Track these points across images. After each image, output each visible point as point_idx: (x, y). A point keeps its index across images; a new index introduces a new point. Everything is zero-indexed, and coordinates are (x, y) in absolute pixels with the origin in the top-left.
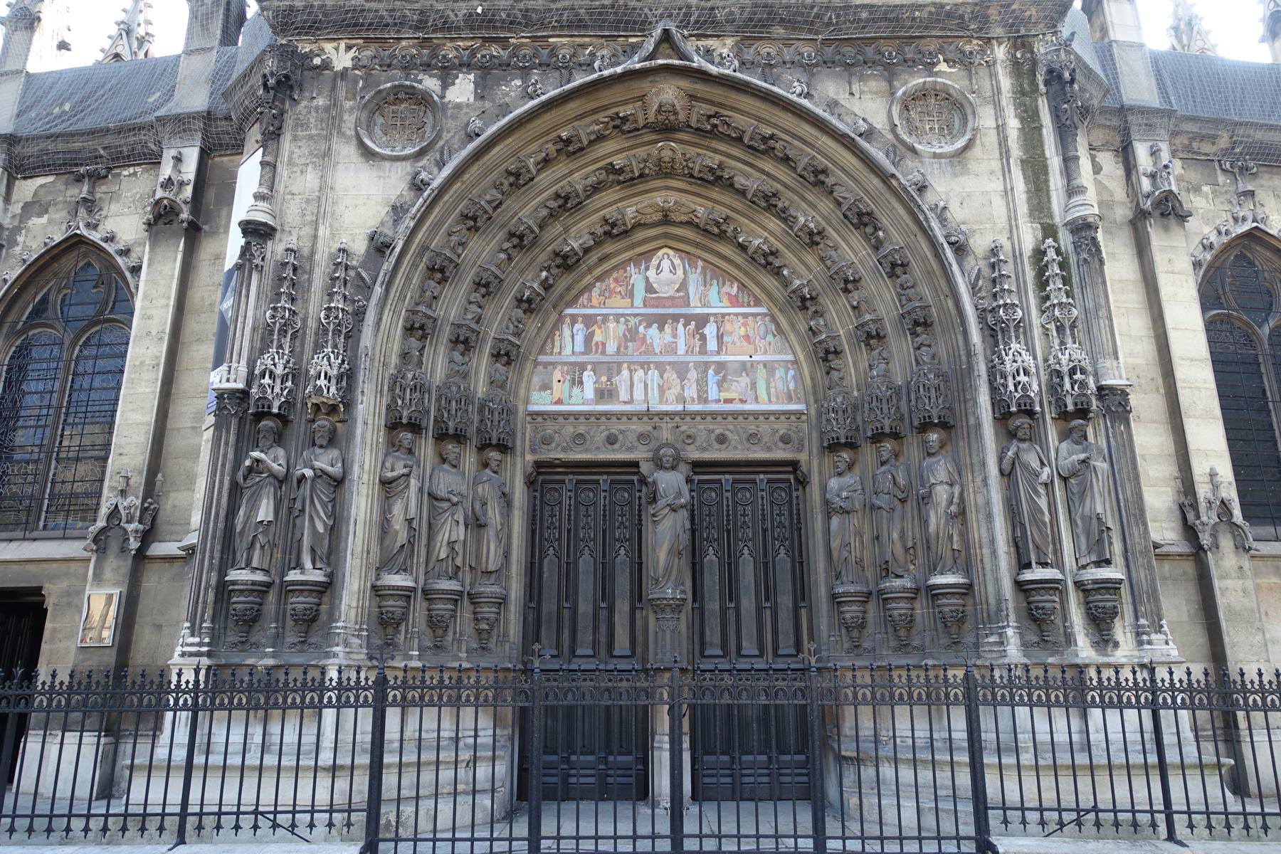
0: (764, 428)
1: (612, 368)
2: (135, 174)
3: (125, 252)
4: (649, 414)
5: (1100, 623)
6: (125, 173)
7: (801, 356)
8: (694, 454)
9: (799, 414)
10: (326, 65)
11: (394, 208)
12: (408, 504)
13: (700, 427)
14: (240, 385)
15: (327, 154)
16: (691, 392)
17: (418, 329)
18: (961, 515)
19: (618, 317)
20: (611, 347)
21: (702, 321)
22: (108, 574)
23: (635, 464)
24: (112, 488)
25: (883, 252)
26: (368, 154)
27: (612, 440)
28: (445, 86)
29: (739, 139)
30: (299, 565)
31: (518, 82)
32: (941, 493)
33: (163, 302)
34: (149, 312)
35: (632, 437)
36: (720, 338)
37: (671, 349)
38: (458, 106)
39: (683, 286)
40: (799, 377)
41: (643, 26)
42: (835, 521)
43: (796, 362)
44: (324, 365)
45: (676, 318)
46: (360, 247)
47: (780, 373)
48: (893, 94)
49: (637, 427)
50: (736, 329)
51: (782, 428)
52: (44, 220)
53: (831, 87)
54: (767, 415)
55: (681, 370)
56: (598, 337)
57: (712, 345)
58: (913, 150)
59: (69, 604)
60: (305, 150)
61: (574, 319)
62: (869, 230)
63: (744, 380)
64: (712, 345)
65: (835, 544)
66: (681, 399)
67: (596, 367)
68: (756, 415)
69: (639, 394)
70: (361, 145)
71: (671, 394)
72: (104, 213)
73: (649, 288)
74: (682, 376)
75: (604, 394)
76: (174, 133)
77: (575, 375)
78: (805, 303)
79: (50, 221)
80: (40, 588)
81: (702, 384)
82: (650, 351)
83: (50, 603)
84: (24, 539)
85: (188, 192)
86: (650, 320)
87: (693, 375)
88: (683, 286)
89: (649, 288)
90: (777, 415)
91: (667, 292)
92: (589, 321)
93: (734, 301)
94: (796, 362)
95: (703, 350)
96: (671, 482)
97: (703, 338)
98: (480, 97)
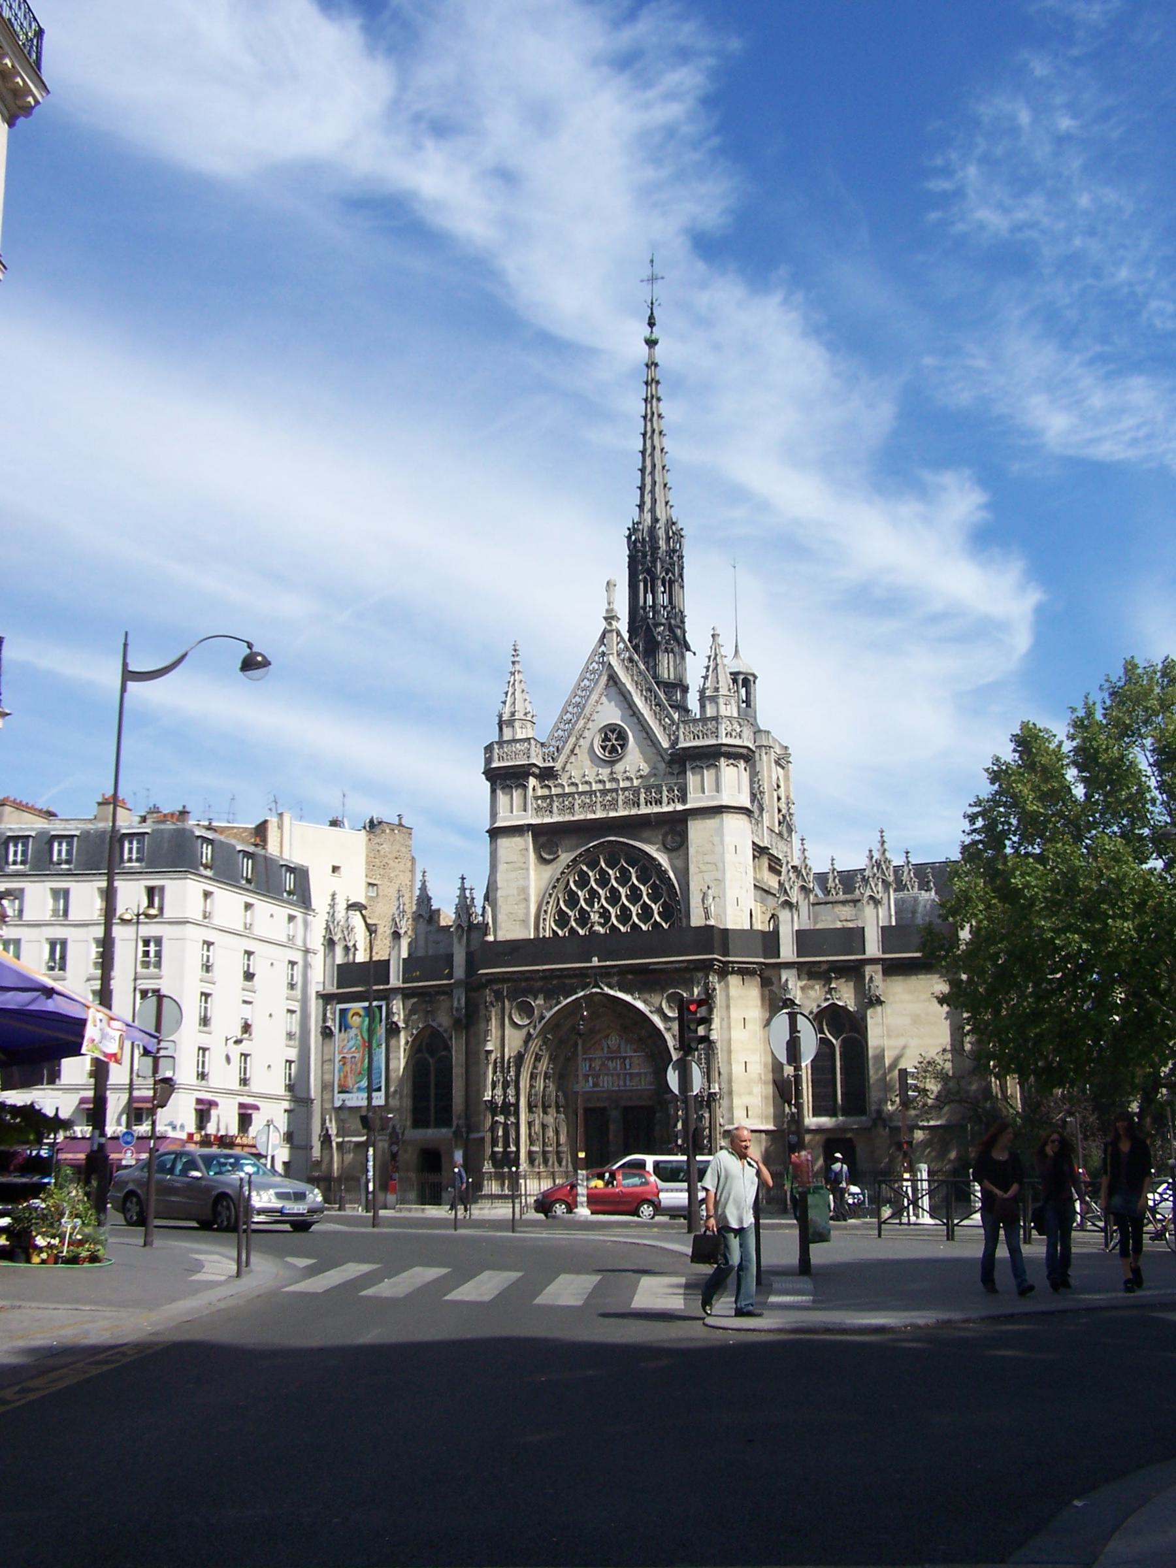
1: (597, 1076)
3: (446, 1031)
12: (537, 1127)
14: (489, 1098)
16: (621, 1083)
17: (533, 1077)
20: (597, 1068)
21: (625, 1058)
30: (509, 1147)
37: (615, 1069)
39: (619, 1046)
44: (511, 1091)
45: (617, 1058)
50: (636, 1061)
52: (416, 1016)
53: (647, 996)
55: (618, 1075)
57: (628, 1067)
61: (585, 1059)
64: (628, 1067)
66: (619, 1086)
67: (594, 1076)
69: (606, 1085)
71: (616, 1084)
73: (609, 1047)
74: (619, 1078)
75: (595, 1085)
77: (586, 1076)
82: (609, 1070)
86: (609, 1059)
87: (622, 1077)
88: (619, 1046)
89: (609, 1047)
92: (591, 1059)
93: (635, 1052)
95: (625, 1069)
96: (615, 1114)
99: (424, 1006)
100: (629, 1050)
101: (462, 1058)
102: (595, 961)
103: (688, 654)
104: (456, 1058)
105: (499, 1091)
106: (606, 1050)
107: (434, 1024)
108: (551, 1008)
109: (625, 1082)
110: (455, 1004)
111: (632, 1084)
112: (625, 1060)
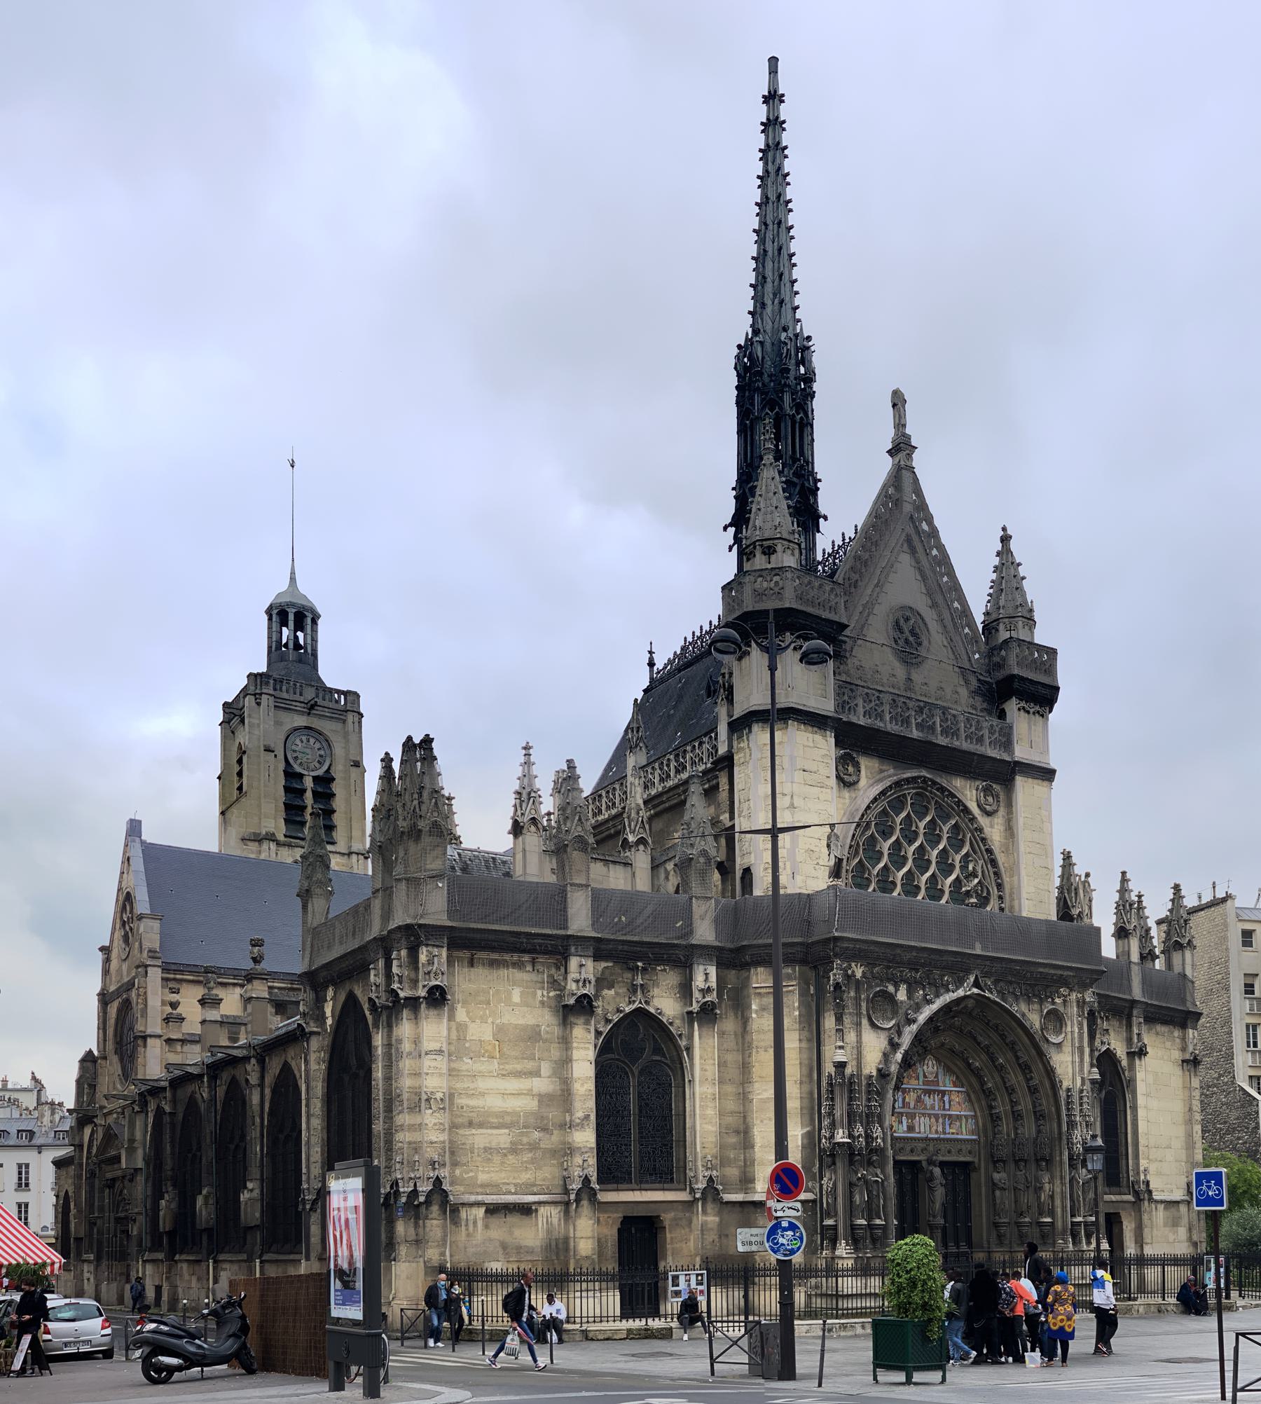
0: (964, 1147)
1: (911, 1116)
2: (665, 970)
3: (671, 1024)
4: (927, 1139)
5: (1088, 1237)
6: (659, 968)
7: (979, 1114)
8: (941, 1158)
9: (974, 1140)
10: (853, 975)
11: (885, 1054)
13: (942, 1146)
15: (859, 1024)
16: (940, 1129)
18: (1052, 1197)
19: (914, 1089)
20: (912, 1106)
21: (943, 1093)
22: (709, 1211)
23: (919, 1162)
24: (703, 1166)
25: (1032, 1083)
26: (873, 1025)
27: (912, 1151)
28: (896, 992)
29: (988, 1024)
31: (921, 992)
32: (1047, 1186)
33: (712, 1062)
34: (705, 1067)
35: (919, 1149)
36: (950, 1102)
37: (933, 1108)
38: (902, 1002)
39: (937, 1076)
40: (977, 1123)
41: (968, 972)
42: (998, 1193)
43: (975, 1116)
45: (934, 1091)
46: (874, 1073)
47: (970, 1120)
48: (1042, 1012)
49: (921, 1145)
51: (969, 1147)
52: (612, 992)
53: (1023, 1007)
54: (965, 1140)
55: (937, 1117)
56: (907, 1100)
57: (947, 1107)
58: (1047, 1040)
59: (677, 1225)
60: (849, 1021)
62: (1027, 1071)
63: (958, 1123)
65: (998, 1202)
66: (937, 1132)
68: (961, 1140)
69: (922, 1130)
70: (870, 1020)
72: (651, 994)
73: (925, 1076)
74: (937, 1121)
75: (911, 1128)
76: (701, 956)
78: (988, 1094)
79: (617, 993)
80: (658, 1217)
81: (944, 1124)
82: (925, 1108)
83: (667, 1224)
84: (640, 1190)
85: (715, 992)
88: (937, 1076)
89: (925, 1076)
90: (968, 1140)
91: (931, 1078)
93: (955, 1086)
94: (975, 1116)
97: (944, 1102)
98: (909, 998)
99: (628, 975)
100: (947, 1081)
101: (713, 1070)
102: (978, 951)
103: (818, 535)
104: (702, 1070)
105: (859, 1130)
106: (921, 1078)
107: (652, 1011)
108: (918, 1008)
109: (944, 1128)
110: (699, 981)
111: (952, 1132)
112: (943, 1096)
